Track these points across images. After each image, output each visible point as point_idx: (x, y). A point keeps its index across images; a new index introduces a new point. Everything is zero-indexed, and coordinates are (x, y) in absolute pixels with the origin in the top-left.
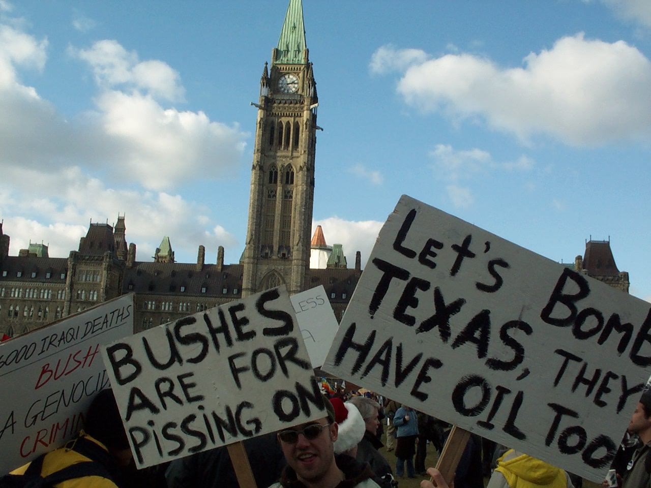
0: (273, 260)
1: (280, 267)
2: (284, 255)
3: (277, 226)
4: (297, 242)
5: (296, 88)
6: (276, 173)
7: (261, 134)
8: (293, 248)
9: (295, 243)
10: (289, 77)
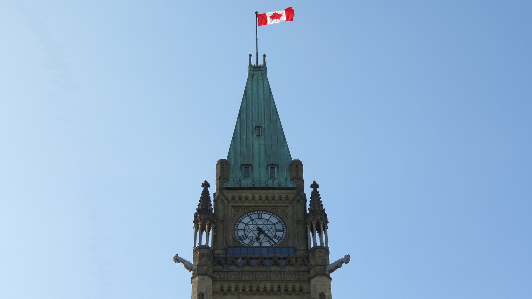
5: (280, 239)
10: (260, 218)
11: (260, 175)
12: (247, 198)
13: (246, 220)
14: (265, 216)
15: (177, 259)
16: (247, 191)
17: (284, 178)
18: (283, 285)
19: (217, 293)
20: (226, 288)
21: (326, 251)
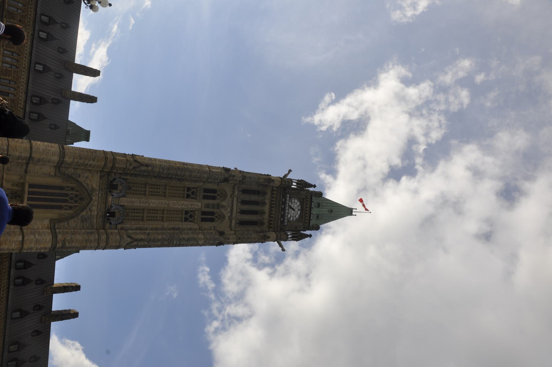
0: (107, 198)
1: (95, 209)
2: (113, 214)
3: (155, 203)
4: (134, 236)
6: (214, 198)
8: (122, 229)
9: (131, 231)
11: (315, 211)
12: (307, 204)
13: (298, 204)
14: (299, 212)
15: (290, 171)
17: (313, 222)
18: (273, 219)
20: (274, 192)
21: (286, 240)
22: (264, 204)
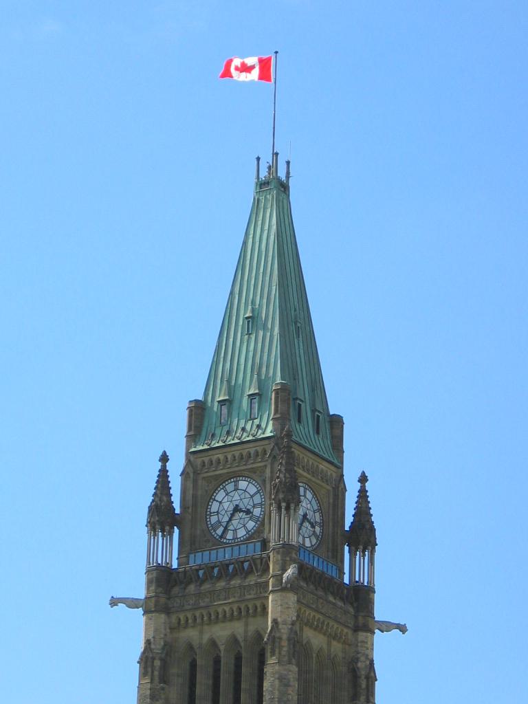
7: (148, 692)
10: (236, 489)
12: (218, 461)
13: (220, 495)
14: (243, 484)
15: (114, 602)
16: (217, 451)
19: (174, 629)
22: (213, 643)
